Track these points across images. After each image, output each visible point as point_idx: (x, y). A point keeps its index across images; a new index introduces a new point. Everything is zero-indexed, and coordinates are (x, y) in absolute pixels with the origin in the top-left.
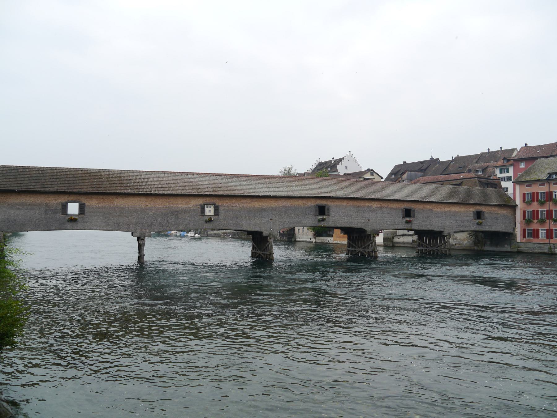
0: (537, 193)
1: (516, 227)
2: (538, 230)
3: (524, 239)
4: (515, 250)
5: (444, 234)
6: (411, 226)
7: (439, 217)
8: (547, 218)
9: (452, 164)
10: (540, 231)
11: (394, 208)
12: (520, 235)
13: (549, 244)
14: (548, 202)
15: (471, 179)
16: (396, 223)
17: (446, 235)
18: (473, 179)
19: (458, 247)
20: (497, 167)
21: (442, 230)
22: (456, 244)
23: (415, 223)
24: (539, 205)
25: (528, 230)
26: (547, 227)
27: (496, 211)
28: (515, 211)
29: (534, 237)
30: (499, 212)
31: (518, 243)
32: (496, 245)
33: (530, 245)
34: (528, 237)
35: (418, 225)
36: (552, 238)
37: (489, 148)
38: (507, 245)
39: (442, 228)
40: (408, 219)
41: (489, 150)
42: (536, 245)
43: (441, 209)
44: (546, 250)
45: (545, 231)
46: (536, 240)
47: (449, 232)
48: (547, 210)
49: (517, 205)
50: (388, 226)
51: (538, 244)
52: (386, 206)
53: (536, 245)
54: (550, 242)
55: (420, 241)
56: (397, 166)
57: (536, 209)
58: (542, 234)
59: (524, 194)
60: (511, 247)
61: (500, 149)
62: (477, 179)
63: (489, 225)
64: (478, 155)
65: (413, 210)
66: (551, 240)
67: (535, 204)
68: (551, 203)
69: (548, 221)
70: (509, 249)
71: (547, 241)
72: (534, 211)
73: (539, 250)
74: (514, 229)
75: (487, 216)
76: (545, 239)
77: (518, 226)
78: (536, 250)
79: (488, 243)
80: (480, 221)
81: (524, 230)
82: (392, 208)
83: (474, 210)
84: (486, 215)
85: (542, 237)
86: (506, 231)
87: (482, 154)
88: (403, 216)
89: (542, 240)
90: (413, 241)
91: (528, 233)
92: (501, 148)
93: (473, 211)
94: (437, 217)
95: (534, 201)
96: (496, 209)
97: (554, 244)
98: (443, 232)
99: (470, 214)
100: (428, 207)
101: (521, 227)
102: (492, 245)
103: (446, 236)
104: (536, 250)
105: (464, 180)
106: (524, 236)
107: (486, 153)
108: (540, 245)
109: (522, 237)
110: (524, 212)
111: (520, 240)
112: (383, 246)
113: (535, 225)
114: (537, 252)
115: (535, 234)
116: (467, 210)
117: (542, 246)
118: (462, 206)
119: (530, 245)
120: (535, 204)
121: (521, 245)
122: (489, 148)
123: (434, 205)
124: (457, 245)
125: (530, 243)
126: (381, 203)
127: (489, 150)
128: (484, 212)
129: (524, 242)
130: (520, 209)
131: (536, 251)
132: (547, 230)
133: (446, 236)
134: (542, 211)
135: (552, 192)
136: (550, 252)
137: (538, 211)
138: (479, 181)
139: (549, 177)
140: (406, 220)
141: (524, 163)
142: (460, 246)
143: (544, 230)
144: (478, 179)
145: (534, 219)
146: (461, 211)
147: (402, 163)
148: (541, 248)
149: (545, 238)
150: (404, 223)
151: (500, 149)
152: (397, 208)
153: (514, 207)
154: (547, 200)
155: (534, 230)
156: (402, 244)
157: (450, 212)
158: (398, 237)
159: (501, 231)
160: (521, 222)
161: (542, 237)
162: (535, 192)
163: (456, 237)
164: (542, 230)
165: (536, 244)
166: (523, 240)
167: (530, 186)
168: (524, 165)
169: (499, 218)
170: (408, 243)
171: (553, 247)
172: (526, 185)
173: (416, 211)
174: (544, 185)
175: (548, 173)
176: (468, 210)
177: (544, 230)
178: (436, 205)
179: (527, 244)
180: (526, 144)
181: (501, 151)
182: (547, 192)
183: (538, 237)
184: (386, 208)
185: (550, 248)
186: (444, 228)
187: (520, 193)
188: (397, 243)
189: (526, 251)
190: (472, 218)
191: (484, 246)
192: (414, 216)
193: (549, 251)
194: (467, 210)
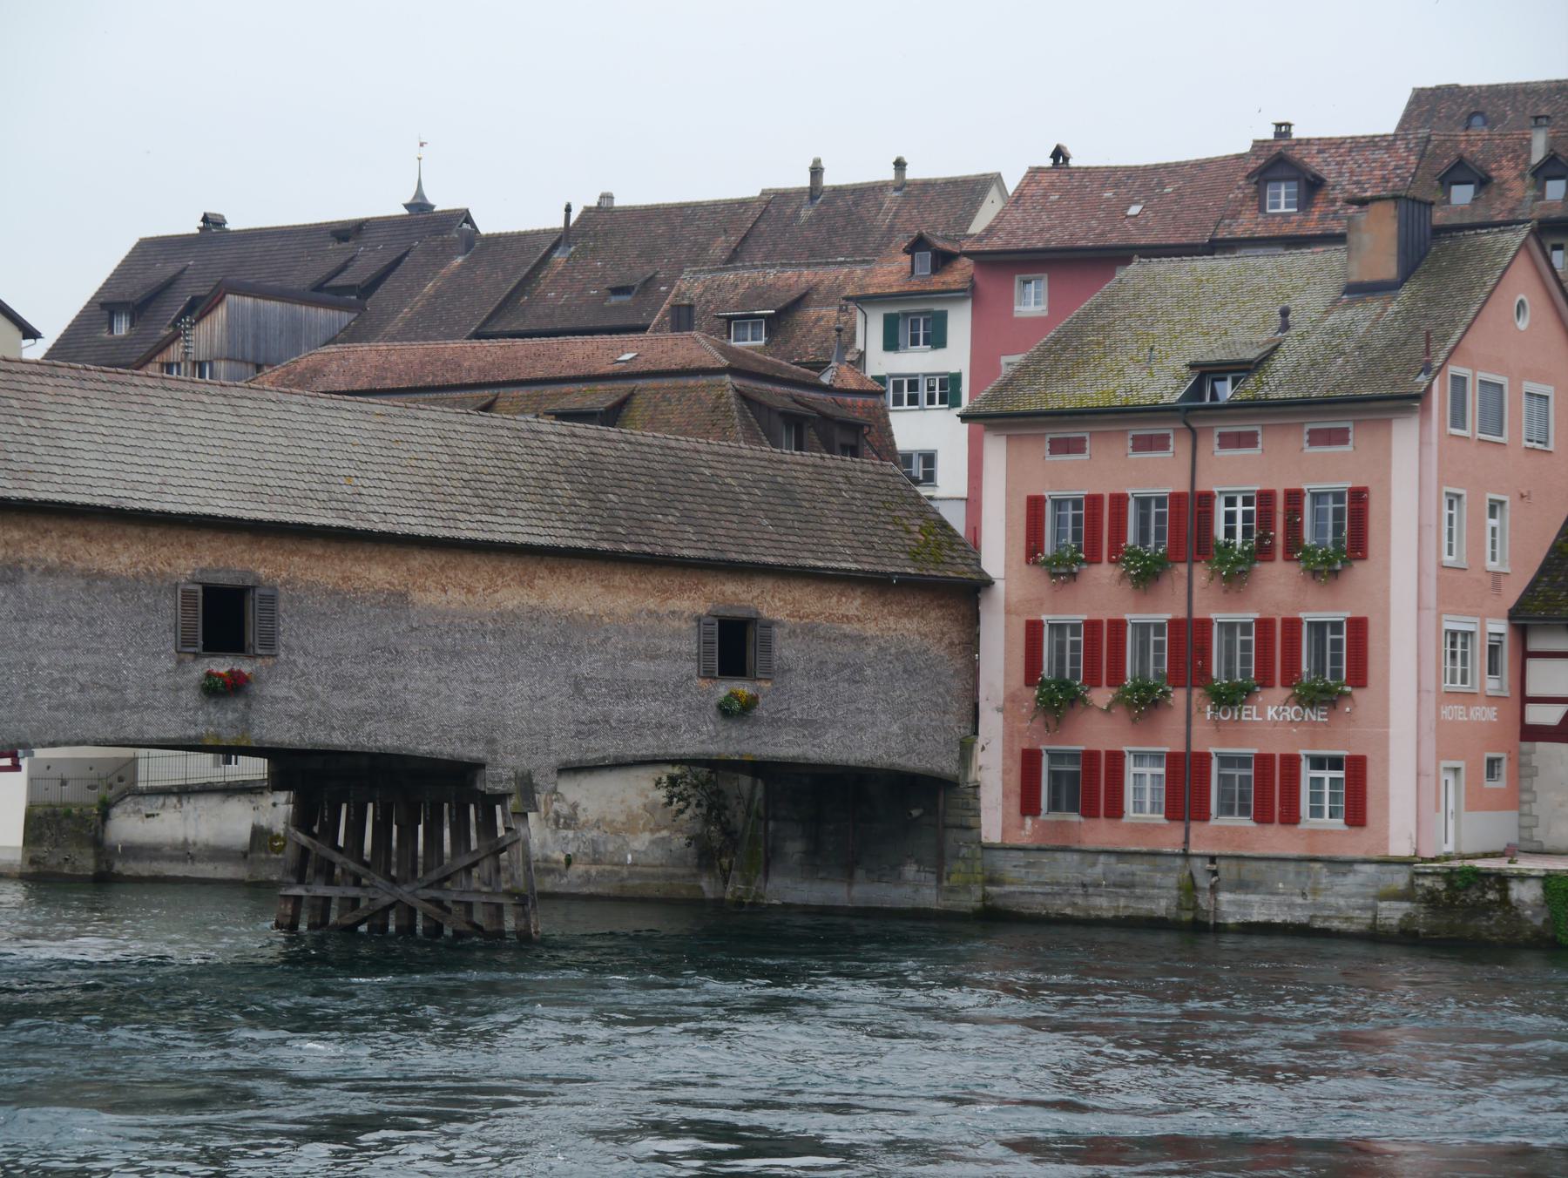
0: (1119, 501)
1: (981, 740)
2: (1116, 759)
3: (1029, 821)
4: (970, 901)
5: (489, 783)
6: (245, 719)
7: (456, 654)
8: (1178, 677)
9: (559, 257)
10: (1130, 768)
11: (116, 579)
12: (1005, 795)
13: (1179, 862)
14: (1182, 568)
15: (691, 382)
16: (132, 695)
17: (500, 788)
18: (703, 381)
19: (587, 879)
20: (866, 300)
21: (475, 752)
22: (569, 861)
23: (277, 693)
24: (1128, 586)
25: (1055, 757)
26: (1172, 743)
27: (848, 619)
28: (974, 620)
29: (1090, 812)
30: (871, 629)
31: (991, 847)
32: (848, 869)
33: (1065, 868)
34: (1055, 806)
35: (295, 708)
36: (1204, 816)
37: (817, 162)
38: (919, 862)
39: (473, 740)
40: (222, 665)
41: (816, 171)
42: (1099, 869)
43: (470, 590)
44: (1163, 903)
45: (1162, 771)
46: (1100, 833)
47: (525, 764)
48: (1171, 622)
49: (988, 583)
50: (61, 715)
51: (1113, 860)
52: (52, 557)
53: (1099, 869)
54: (1187, 842)
55: (309, 833)
56: (149, 249)
57: (1105, 615)
58: (1138, 791)
59: (1035, 506)
60: (939, 880)
61: (889, 174)
62: (727, 378)
63: (804, 724)
64: (743, 203)
65: (263, 598)
66: (1196, 827)
67: (1105, 573)
68: (1201, 573)
69: (1178, 696)
70: (929, 897)
71: (1171, 839)
72: (1092, 627)
74: (966, 750)
75: (786, 653)
76: (1157, 826)
77: (992, 724)
78: (1103, 902)
79: (794, 848)
80: (744, 688)
81: (1030, 761)
82: (102, 575)
83: (702, 608)
84: (786, 650)
85: (1139, 806)
86: (913, 763)
87: (775, 201)
88: (185, 643)
89: (1137, 828)
90: (258, 833)
91: (1055, 776)
92: (900, 165)
93: (698, 619)
94: (439, 653)
95: (1094, 558)
96: (852, 604)
97: (1213, 859)
98: (478, 766)
99: (676, 635)
100: (377, 573)
101: (1009, 736)
102: (815, 864)
103: (502, 798)
104: (1103, 902)
105: (640, 383)
106: (1029, 805)
107: (799, 192)
108: (1123, 867)
109: (1015, 808)
110: (1033, 630)
111: (1004, 831)
112: (23, 878)
114: (1110, 914)
116: (652, 603)
117: (1139, 868)
118: (619, 578)
119: (1065, 868)
120: (1105, 573)
121: (1010, 866)
122: (817, 162)
123: (419, 560)
124: (578, 868)
125: (1065, 849)
126: (17, 535)
127: (816, 171)
128: (770, 624)
130: (1008, 612)
131: (1103, 905)
132: (1173, 760)
133: (502, 798)
134: (1143, 628)
135: (1206, 500)
136: (1187, 916)
137: (1118, 626)
138: (742, 396)
139: (1196, 392)
140: (209, 675)
141: (1044, 285)
142: (601, 874)
143: (1156, 757)
144: (737, 382)
145: (1093, 680)
146: (611, 614)
147: (192, 226)
148: (1132, 885)
149: (1160, 818)
150: (190, 697)
151: (889, 174)
152: (136, 578)
153: (976, 587)
154: (1175, 555)
155: (1090, 757)
156: (172, 859)
157: (535, 615)
158: (147, 805)
159: (878, 764)
160: (1012, 698)
161: (1139, 806)
162: (1106, 489)
163: (575, 806)
164: (1139, 757)
165: (1102, 858)
166: (1022, 827)
167: (1074, 446)
168: (1044, 297)
169: (868, 672)
170: (218, 854)
171: (1204, 882)
172: (1052, 442)
173: (282, 605)
174: (1159, 443)
175: (1192, 366)
176: (663, 610)
177: (1156, 757)
178: (440, 559)
179: (1045, 858)
180: (1059, 154)
181: (901, 185)
182: (1176, 498)
183: (1115, 810)
184: (49, 571)
185: (1190, 888)
186: (492, 741)
187: (1009, 494)
188: (134, 851)
189: (1037, 906)
190: (690, 667)
192: (270, 643)
193: (1180, 906)
194: (652, 603)
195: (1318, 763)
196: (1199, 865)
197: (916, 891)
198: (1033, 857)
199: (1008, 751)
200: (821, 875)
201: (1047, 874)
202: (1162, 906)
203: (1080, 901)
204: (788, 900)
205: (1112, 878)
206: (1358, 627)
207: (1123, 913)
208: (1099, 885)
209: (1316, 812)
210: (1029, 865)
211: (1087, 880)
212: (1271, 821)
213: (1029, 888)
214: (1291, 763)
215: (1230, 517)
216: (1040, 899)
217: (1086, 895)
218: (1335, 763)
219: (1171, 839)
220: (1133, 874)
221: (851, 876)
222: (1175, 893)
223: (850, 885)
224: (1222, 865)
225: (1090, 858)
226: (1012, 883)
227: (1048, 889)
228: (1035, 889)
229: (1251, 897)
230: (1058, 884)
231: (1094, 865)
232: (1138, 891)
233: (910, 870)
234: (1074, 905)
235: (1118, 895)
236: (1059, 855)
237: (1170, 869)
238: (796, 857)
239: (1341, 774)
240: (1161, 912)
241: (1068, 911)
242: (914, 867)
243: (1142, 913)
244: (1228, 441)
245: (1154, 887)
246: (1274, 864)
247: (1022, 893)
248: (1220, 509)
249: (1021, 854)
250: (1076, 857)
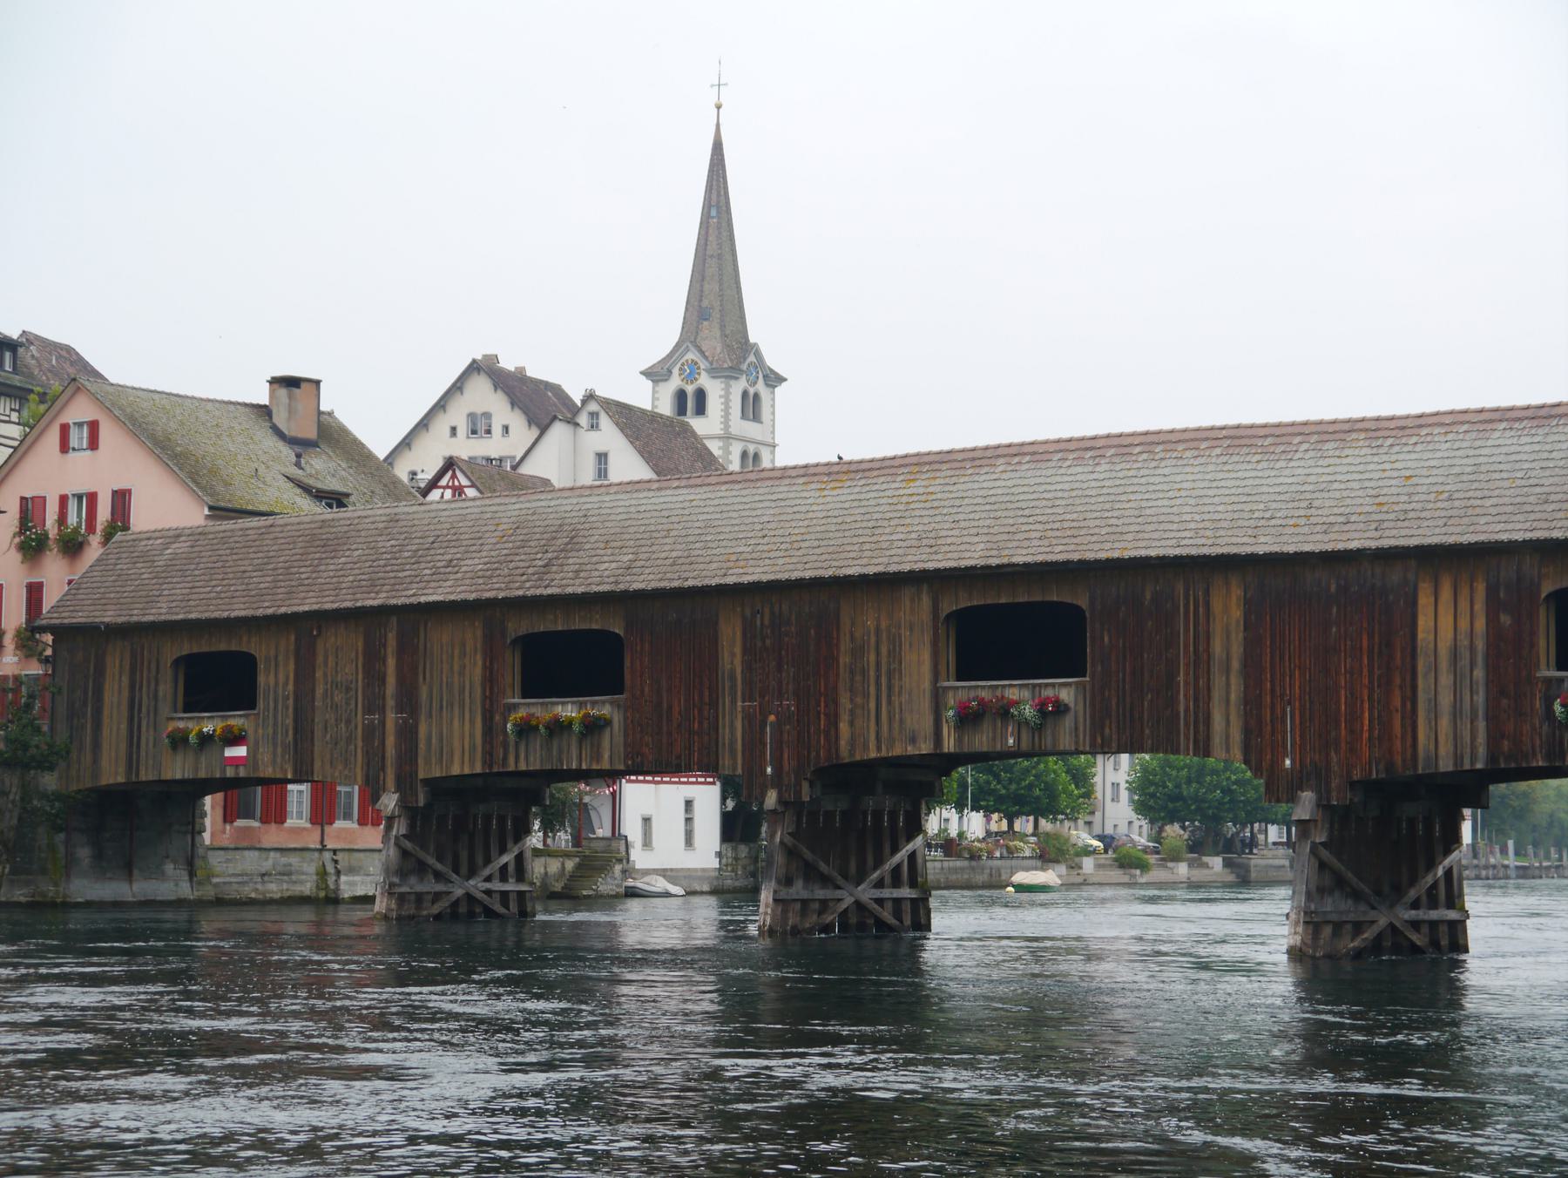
3: (228, 827)
13: (316, 854)
32: (128, 869)
33: (250, 862)
38: (175, 862)
42: (270, 862)
44: (308, 885)
46: (272, 836)
51: (278, 855)
70: (185, 890)
73: (285, 886)
76: (305, 829)
78: (273, 887)
79: (84, 853)
89: (297, 831)
102: (103, 865)
104: (273, 887)
108: (284, 860)
112: (546, 873)
114: (277, 896)
117: (293, 860)
121: (215, 860)
129: (226, 844)
131: (274, 889)
136: (322, 894)
148: (289, 874)
165: (272, 854)
171: (330, 869)
179: (238, 855)
185: (322, 874)
189: (233, 893)
191: (68, 876)
193: (317, 887)
196: (327, 856)
197: (177, 885)
198: (230, 855)
200: (108, 875)
201: (239, 869)
202: (307, 887)
203: (259, 887)
204: (89, 898)
205: (279, 869)
207: (287, 894)
208: (270, 875)
210: (228, 861)
211: (263, 871)
212: (366, 824)
213: (228, 879)
216: (235, 887)
217: (263, 882)
219: (313, 841)
220: (290, 865)
221: (130, 874)
222: (315, 877)
223: (131, 882)
224: (339, 857)
225: (264, 855)
226: (218, 876)
227: (240, 879)
228: (233, 880)
229: (357, 878)
230: (247, 875)
231: (267, 859)
232: (294, 878)
233: (169, 868)
234: (256, 890)
235: (282, 881)
236: (246, 853)
237: (312, 860)
238: (87, 861)
240: (307, 893)
241: (253, 895)
242: (172, 866)
243: (297, 893)
245: (303, 874)
246: (368, 854)
247: (224, 883)
249: (222, 853)
250: (256, 853)
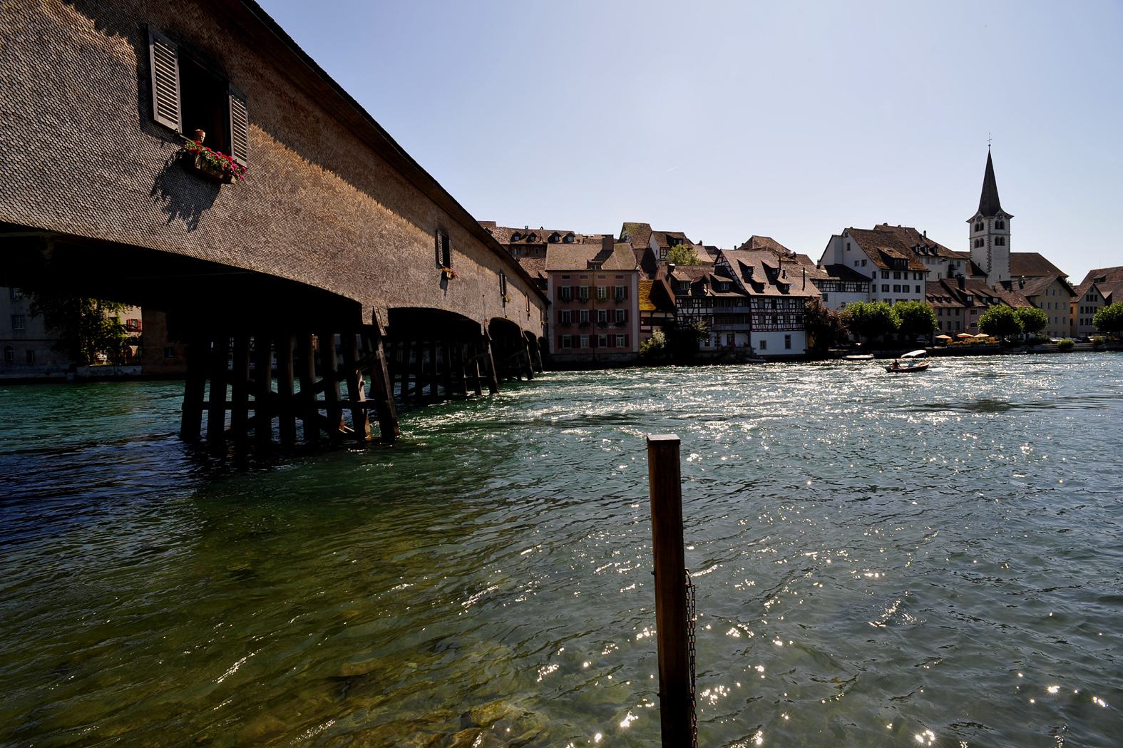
2: (579, 337)
14: (591, 301)
34: (565, 346)
57: (575, 309)
59: (559, 289)
81: (560, 338)
89: (583, 349)
106: (560, 346)
111: (555, 351)
113: (574, 330)
115: (576, 341)
145: (573, 321)
195: (618, 336)
199: (555, 336)
206: (626, 311)
209: (619, 345)
214: (614, 336)
215: (600, 291)
218: (622, 336)
239: (623, 338)
244: (600, 277)
248: (598, 290)
